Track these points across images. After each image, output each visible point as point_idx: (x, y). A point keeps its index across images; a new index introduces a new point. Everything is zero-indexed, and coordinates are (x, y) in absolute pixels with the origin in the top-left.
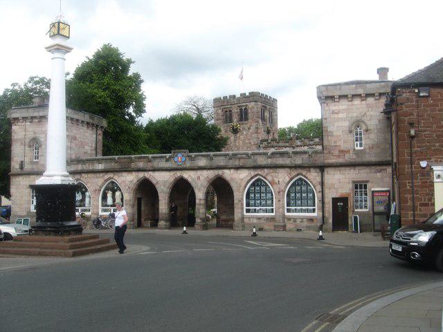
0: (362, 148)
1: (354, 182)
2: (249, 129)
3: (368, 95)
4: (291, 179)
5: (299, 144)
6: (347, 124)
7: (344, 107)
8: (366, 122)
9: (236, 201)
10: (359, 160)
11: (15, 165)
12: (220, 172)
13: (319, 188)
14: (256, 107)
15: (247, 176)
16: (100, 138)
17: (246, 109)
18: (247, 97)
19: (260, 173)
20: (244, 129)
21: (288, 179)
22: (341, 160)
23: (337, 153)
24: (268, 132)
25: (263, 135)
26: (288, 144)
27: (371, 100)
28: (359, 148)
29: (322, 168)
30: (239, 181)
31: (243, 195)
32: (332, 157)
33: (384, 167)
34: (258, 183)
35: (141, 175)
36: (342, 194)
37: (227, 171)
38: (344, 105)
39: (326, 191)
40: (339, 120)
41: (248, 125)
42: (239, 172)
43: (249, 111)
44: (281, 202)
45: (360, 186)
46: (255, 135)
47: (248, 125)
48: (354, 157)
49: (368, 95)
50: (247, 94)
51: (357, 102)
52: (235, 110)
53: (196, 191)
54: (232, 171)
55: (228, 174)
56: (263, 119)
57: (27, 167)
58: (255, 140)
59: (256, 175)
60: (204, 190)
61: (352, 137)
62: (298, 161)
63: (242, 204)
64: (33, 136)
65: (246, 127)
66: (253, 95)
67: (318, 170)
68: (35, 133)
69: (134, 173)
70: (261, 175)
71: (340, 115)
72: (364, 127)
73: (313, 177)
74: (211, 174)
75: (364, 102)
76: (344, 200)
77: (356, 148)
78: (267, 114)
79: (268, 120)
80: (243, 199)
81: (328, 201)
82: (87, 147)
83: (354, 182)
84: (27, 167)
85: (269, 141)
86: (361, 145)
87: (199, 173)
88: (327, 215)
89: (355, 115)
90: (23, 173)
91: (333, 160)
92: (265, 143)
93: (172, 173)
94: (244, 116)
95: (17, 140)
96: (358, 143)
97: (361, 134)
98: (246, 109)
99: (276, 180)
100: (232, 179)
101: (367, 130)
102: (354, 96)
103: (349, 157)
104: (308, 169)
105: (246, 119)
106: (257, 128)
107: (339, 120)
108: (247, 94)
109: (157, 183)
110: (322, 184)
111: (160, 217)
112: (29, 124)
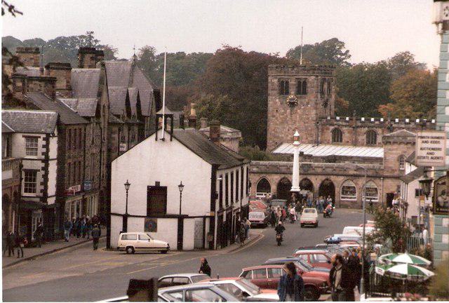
2: (308, 104)
3: (407, 143)
6: (396, 156)
9: (336, 192)
20: (301, 103)
22: (391, 174)
35: (283, 176)
37: (332, 177)
40: (393, 154)
41: (307, 100)
43: (309, 85)
47: (307, 100)
51: (402, 146)
52: (293, 82)
55: (333, 178)
61: (398, 164)
62: (370, 173)
74: (324, 178)
78: (326, 86)
85: (329, 118)
87: (316, 177)
89: (400, 152)
92: (325, 120)
102: (400, 143)
105: (305, 93)
107: (393, 154)
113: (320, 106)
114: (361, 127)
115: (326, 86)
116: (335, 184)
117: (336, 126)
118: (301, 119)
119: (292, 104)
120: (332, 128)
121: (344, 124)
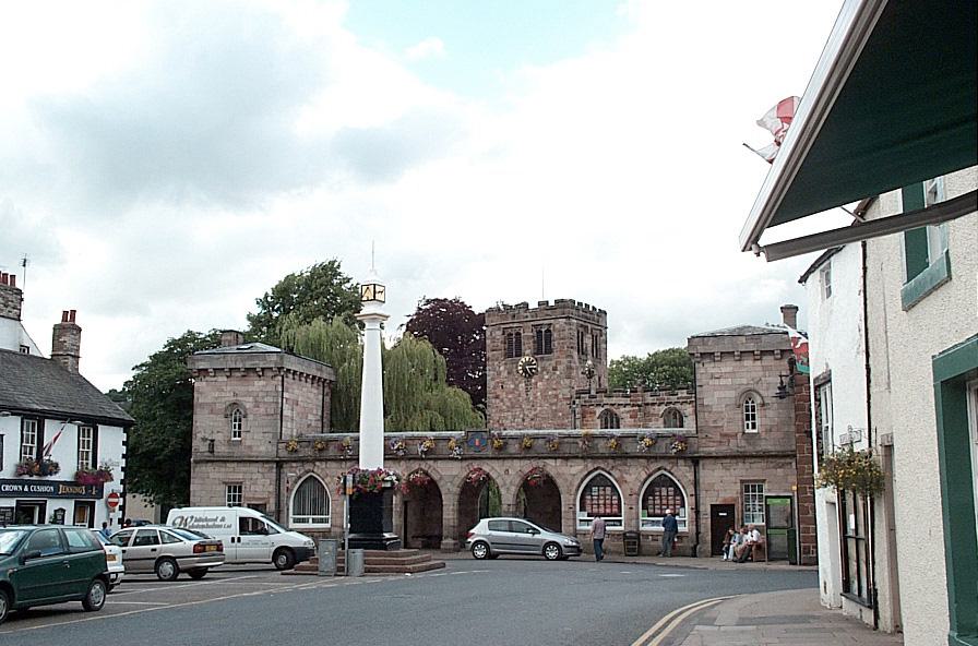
0: (755, 431)
1: (742, 481)
2: (555, 369)
3: (763, 353)
4: (649, 476)
5: (650, 400)
6: (732, 394)
7: (729, 369)
8: (761, 392)
10: (750, 449)
11: (199, 446)
12: (540, 463)
13: (691, 490)
14: (567, 327)
15: (581, 471)
16: (327, 399)
17: (548, 331)
18: (552, 308)
19: (602, 466)
20: (544, 369)
21: (645, 476)
22: (723, 449)
23: (718, 438)
24: (590, 375)
25: (580, 381)
26: (628, 401)
27: (768, 360)
28: (750, 431)
29: (696, 461)
30: (570, 478)
31: (575, 500)
32: (711, 444)
33: (788, 460)
34: (601, 481)
36: (725, 500)
37: (551, 462)
38: (727, 366)
39: (703, 494)
40: (716, 388)
41: (553, 363)
42: (569, 464)
43: (555, 335)
44: (633, 511)
45: (751, 487)
46: (567, 381)
47: (553, 363)
48: (743, 443)
49: (763, 353)
50: (552, 303)
51: (748, 363)
52: (527, 333)
53: (503, 491)
54: (559, 461)
55: (553, 467)
56: (581, 351)
57: (221, 449)
58: (566, 391)
59: (596, 469)
60: (513, 489)
61: (739, 415)
63: (574, 513)
64: (233, 399)
65: (549, 365)
66: (561, 303)
67: (690, 463)
68: (235, 395)
69: (402, 463)
70: (603, 469)
71: (723, 382)
72: (758, 400)
73: (682, 474)
74: (526, 466)
75: (758, 363)
76: (729, 508)
77: (747, 431)
78: (588, 341)
79: (590, 352)
80: (575, 505)
81: (706, 509)
82: (310, 417)
83: (742, 481)
84: (221, 449)
85: (593, 392)
86: (754, 427)
88: (702, 530)
89: (744, 381)
90: (213, 459)
91: (713, 449)
93: (465, 464)
94: (544, 343)
95: (202, 405)
96: (750, 423)
97: (753, 410)
98: (548, 331)
99: (627, 477)
100: (558, 474)
101: (763, 405)
103: (733, 446)
104: (675, 461)
105: (549, 351)
106: (570, 368)
108: (552, 303)
109: (441, 478)
110: (696, 483)
111: (445, 533)
112: (225, 379)
113: (578, 374)
114: (653, 404)
115: (588, 341)
116: (559, 482)
117: (606, 407)
118: (545, 397)
119: (529, 374)
120: (599, 410)
121: (623, 401)
